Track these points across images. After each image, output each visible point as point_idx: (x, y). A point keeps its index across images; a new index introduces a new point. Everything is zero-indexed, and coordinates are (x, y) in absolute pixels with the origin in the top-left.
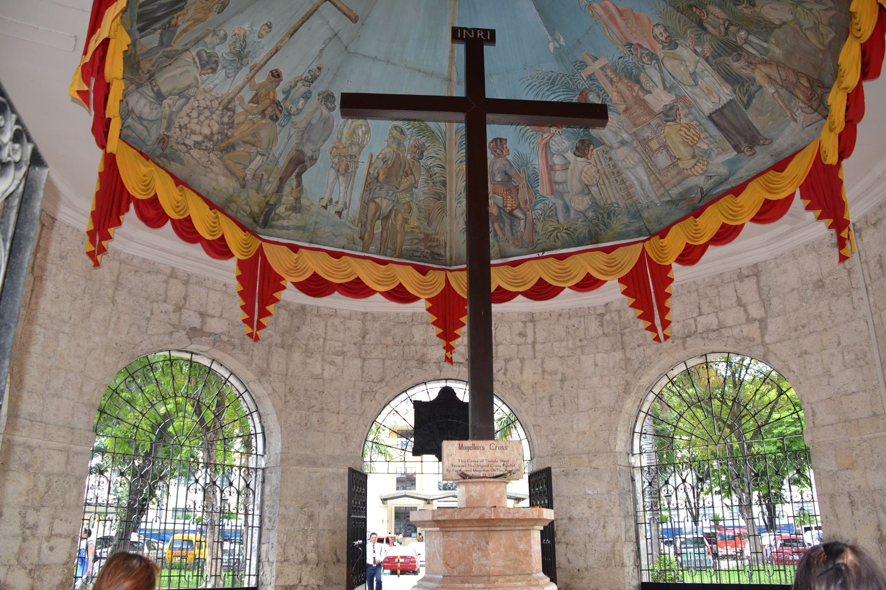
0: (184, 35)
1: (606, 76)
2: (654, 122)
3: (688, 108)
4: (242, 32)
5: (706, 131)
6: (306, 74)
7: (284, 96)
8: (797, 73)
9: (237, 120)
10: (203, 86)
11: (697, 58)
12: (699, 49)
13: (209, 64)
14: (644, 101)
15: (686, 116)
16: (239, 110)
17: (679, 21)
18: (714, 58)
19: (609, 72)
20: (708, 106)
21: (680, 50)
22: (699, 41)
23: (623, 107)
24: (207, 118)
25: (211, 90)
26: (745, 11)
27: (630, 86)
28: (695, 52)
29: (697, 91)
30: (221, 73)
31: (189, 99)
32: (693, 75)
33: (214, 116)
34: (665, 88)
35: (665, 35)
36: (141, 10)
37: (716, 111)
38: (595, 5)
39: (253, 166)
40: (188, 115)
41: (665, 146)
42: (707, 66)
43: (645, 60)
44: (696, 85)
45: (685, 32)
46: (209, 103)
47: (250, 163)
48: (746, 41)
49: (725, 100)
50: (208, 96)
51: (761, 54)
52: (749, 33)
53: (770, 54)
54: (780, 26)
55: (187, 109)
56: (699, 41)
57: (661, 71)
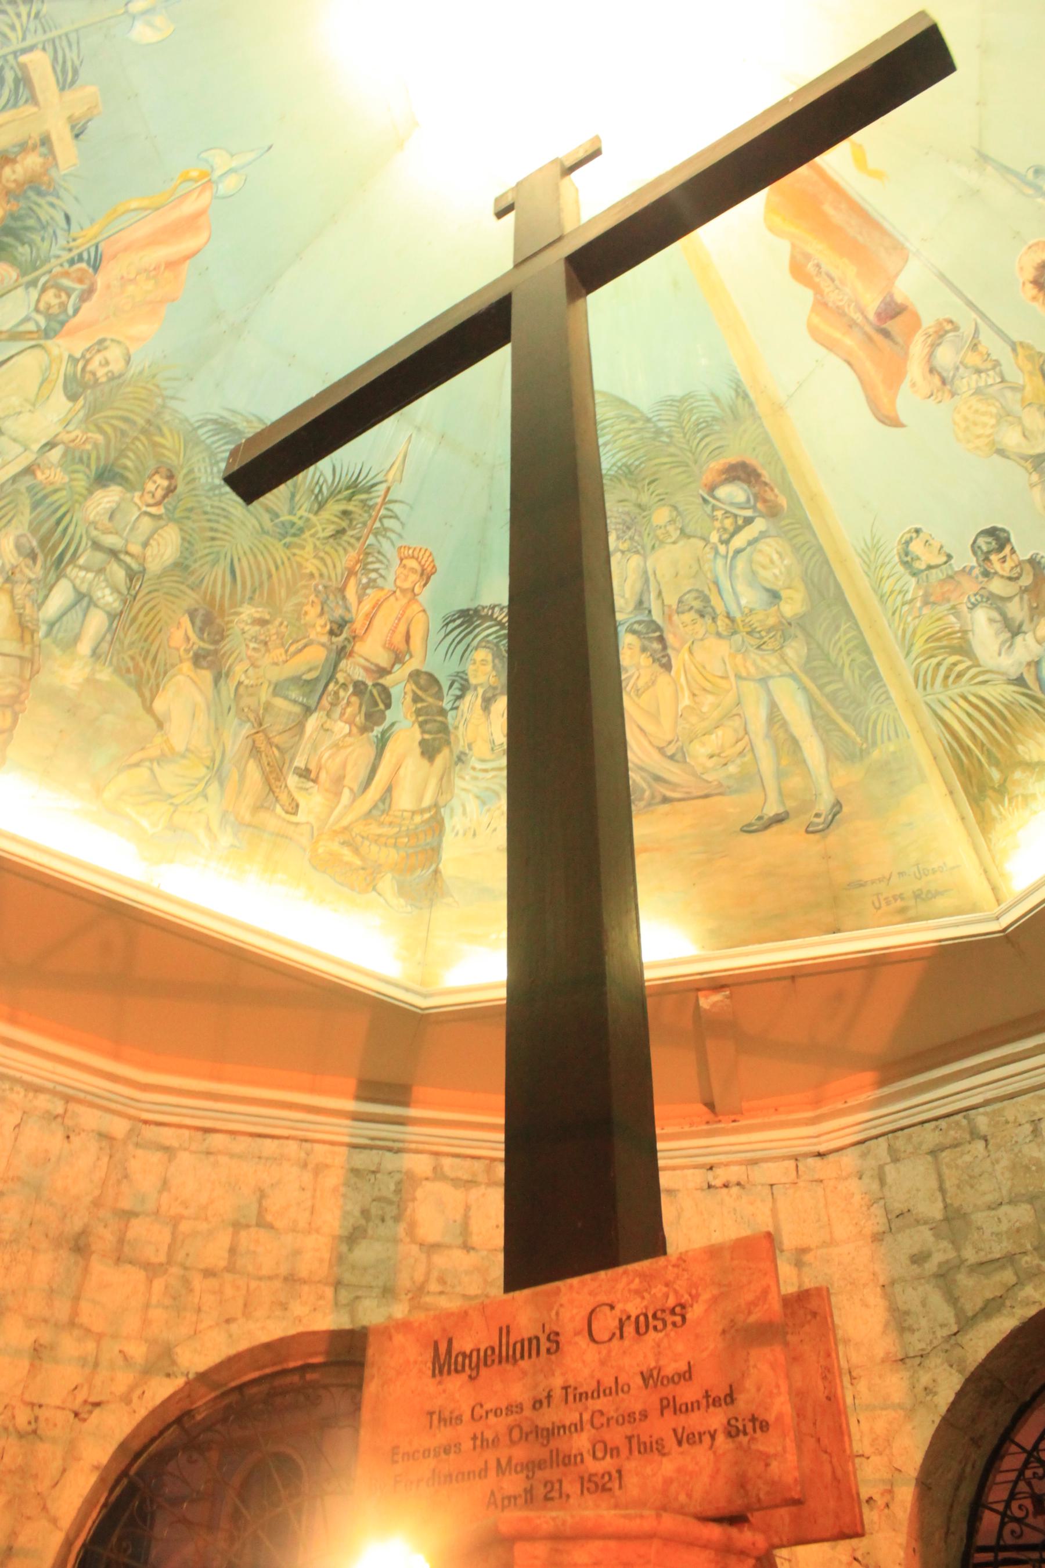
11: (36, 447)
12: (55, 454)
17: (125, 420)
18: (29, 489)
21: (59, 405)
22: (73, 457)
28: (51, 445)
35: (101, 373)
38: (207, 196)
43: (50, 297)
45: (100, 430)
48: (83, 599)
51: (51, 625)
52: (113, 617)
53: (57, 652)
54: (149, 710)
56: (73, 457)
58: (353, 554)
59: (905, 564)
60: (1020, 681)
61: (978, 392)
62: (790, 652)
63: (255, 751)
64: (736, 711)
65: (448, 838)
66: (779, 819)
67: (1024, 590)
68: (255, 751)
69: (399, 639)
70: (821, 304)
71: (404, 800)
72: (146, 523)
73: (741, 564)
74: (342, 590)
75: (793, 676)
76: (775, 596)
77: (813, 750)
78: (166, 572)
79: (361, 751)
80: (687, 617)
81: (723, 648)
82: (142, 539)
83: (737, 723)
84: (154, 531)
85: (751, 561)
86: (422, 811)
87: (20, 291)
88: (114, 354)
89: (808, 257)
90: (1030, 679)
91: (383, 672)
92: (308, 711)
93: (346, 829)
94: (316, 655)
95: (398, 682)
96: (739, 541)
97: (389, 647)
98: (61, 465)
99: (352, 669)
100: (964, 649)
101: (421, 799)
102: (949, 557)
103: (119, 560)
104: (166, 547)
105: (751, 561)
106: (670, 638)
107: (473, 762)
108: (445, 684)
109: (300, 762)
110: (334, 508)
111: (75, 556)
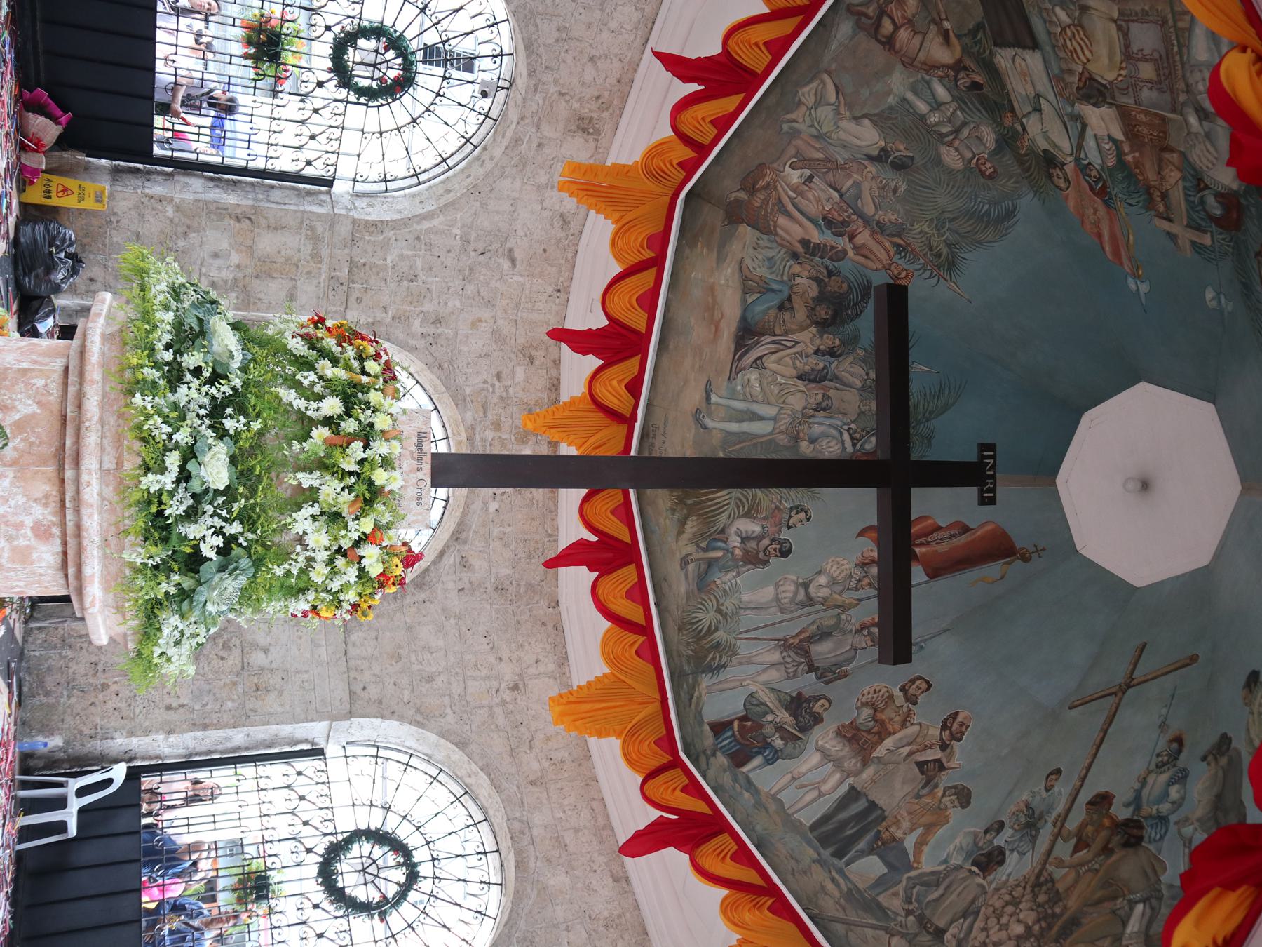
0: (926, 849)
1: (1167, 207)
2: (1127, 100)
3: (1063, 80)
4: (1023, 806)
5: (1049, 33)
6: (1154, 761)
7: (1131, 809)
8: (889, 43)
9: (1061, 887)
10: (993, 886)
11: (1024, 121)
12: (1019, 128)
13: (989, 860)
14: (1126, 135)
15: (1070, 72)
16: (1058, 873)
19: (1161, 208)
20: (1033, 60)
21: (1043, 145)
23: (1167, 155)
24: (1011, 916)
25: (1007, 880)
26: (902, 147)
27: (1137, 167)
28: (1024, 129)
29: (1040, 89)
30: (1012, 859)
31: (977, 913)
32: (1037, 109)
33: (1021, 906)
34: (1084, 126)
36: (816, 833)
37: (1024, 47)
39: (1133, 926)
40: (985, 929)
41: (1128, 55)
42: (1016, 105)
44: (1038, 96)
45: (1026, 155)
46: (1007, 897)
47: (1124, 924)
48: (937, 105)
49: (1009, 52)
50: (1003, 891)
51: (928, 83)
52: (923, 118)
55: (979, 924)
57: (1080, 146)
58: (918, 250)
59: (797, 507)
60: (723, 531)
61: (851, 576)
62: (783, 437)
63: (828, 160)
64: (765, 401)
65: (757, 233)
66: (708, 398)
67: (758, 552)
68: (828, 160)
69: (866, 252)
70: (939, 528)
71: (782, 221)
72: (968, 155)
73: (834, 432)
74: (899, 236)
75: (771, 433)
76: (813, 441)
77: (734, 427)
78: (938, 156)
79: (812, 209)
80: (820, 396)
81: (798, 407)
82: (961, 149)
83: (760, 398)
84: (962, 157)
85: (834, 437)
86: (775, 226)
87: (1100, 162)
88: (1062, 184)
89: (961, 534)
90: (721, 536)
91: (852, 238)
92: (841, 196)
93: (775, 188)
94: (869, 210)
95: (842, 243)
96: (846, 436)
97: (863, 246)
98: (1012, 127)
99: (858, 224)
100: (747, 515)
101: (782, 229)
102: (789, 527)
103: (952, 132)
104: (951, 158)
105: (834, 437)
106: (813, 385)
107: (791, 262)
108: (836, 264)
109: (816, 179)
110: (945, 251)
111: (962, 110)
